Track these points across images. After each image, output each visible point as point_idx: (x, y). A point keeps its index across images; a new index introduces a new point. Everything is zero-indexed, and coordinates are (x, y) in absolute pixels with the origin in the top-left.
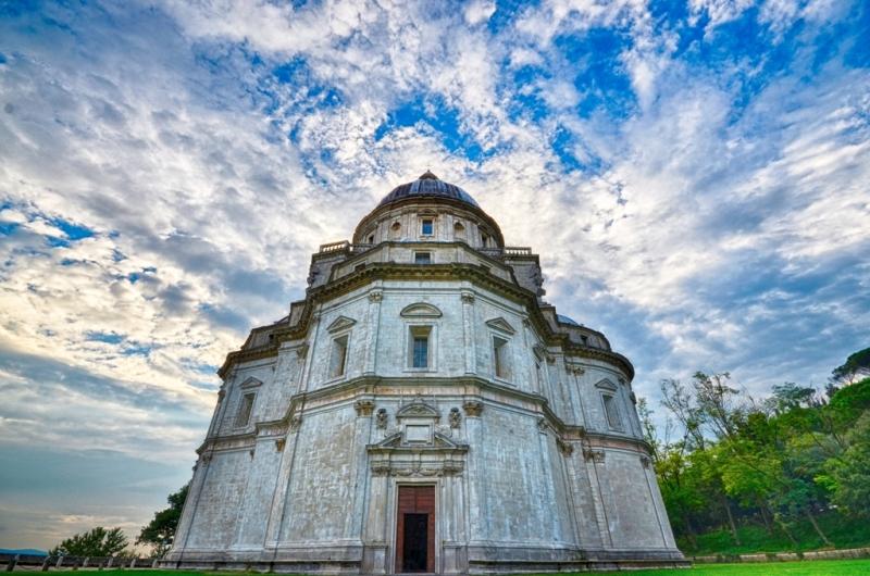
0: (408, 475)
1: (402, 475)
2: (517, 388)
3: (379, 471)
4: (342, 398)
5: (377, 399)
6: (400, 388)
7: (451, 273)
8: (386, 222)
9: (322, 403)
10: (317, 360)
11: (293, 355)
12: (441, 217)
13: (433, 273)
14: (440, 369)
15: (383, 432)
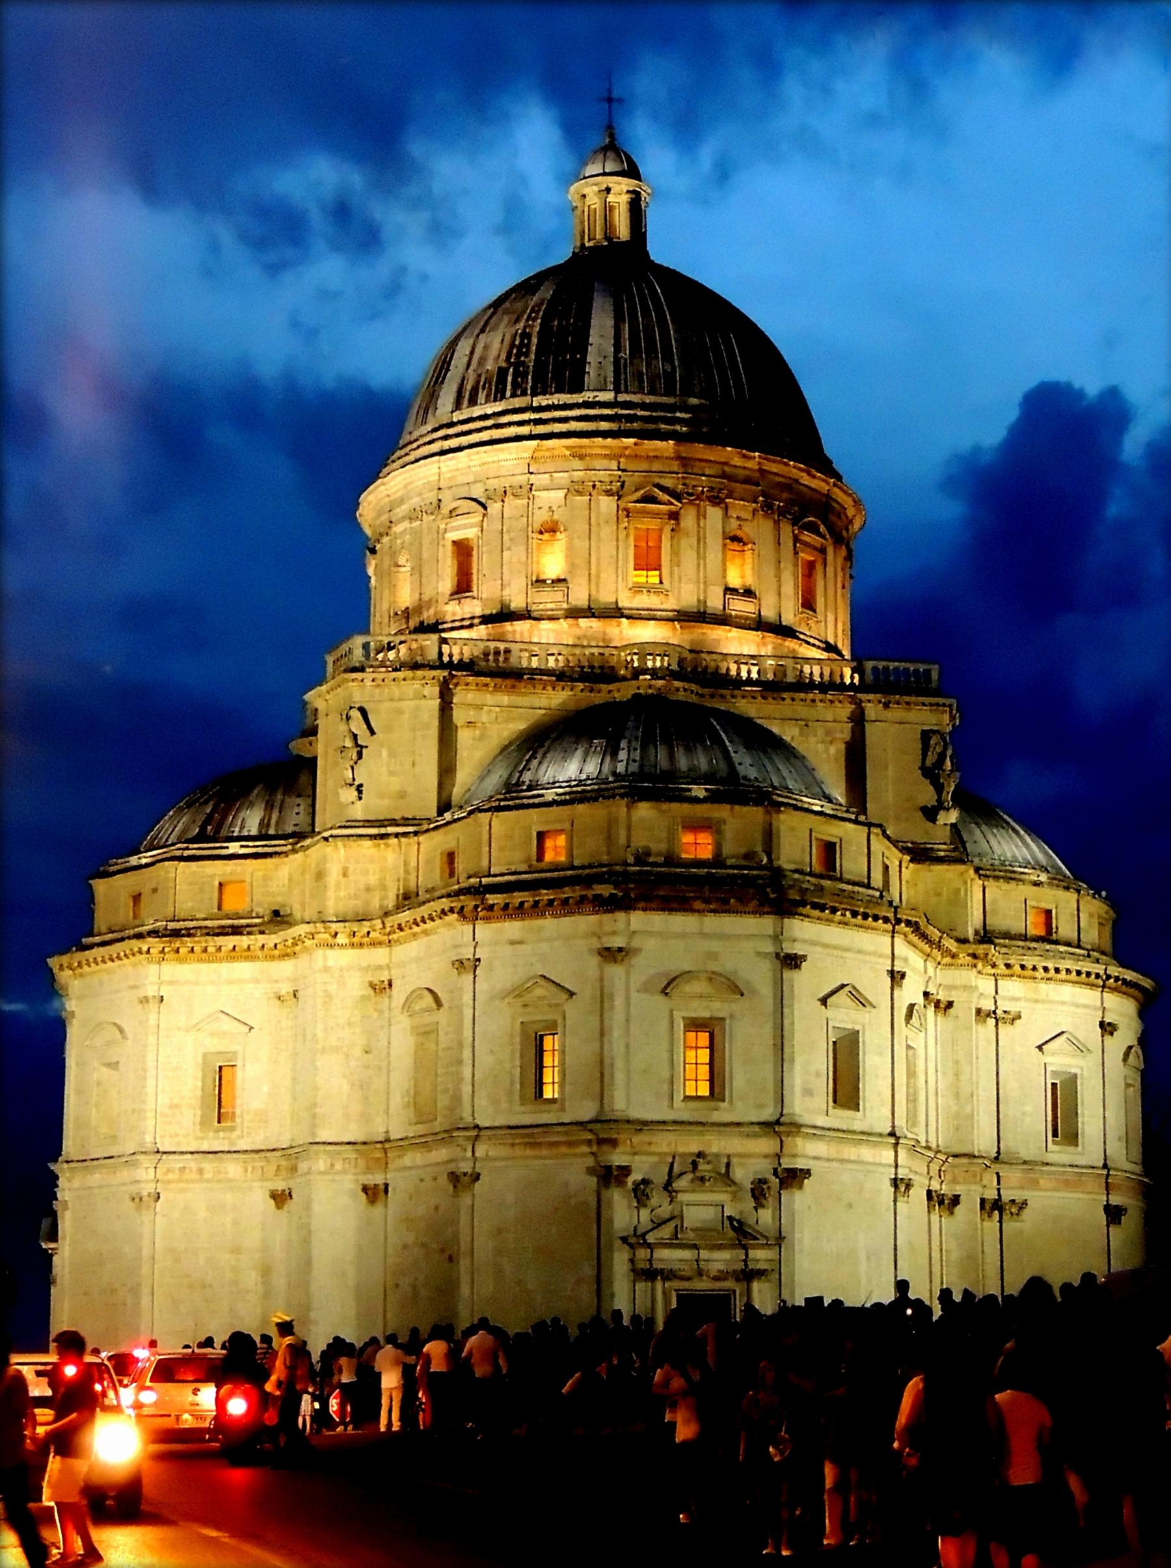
0: (688, 1279)
1: (683, 1278)
2: (866, 1129)
3: (650, 1274)
4: (564, 1150)
5: (636, 1157)
6: (671, 1137)
7: (761, 905)
8: (514, 505)
9: (519, 1151)
10: (485, 1060)
11: (356, 985)
12: (688, 520)
13: (727, 902)
14: (738, 1104)
15: (645, 1214)
